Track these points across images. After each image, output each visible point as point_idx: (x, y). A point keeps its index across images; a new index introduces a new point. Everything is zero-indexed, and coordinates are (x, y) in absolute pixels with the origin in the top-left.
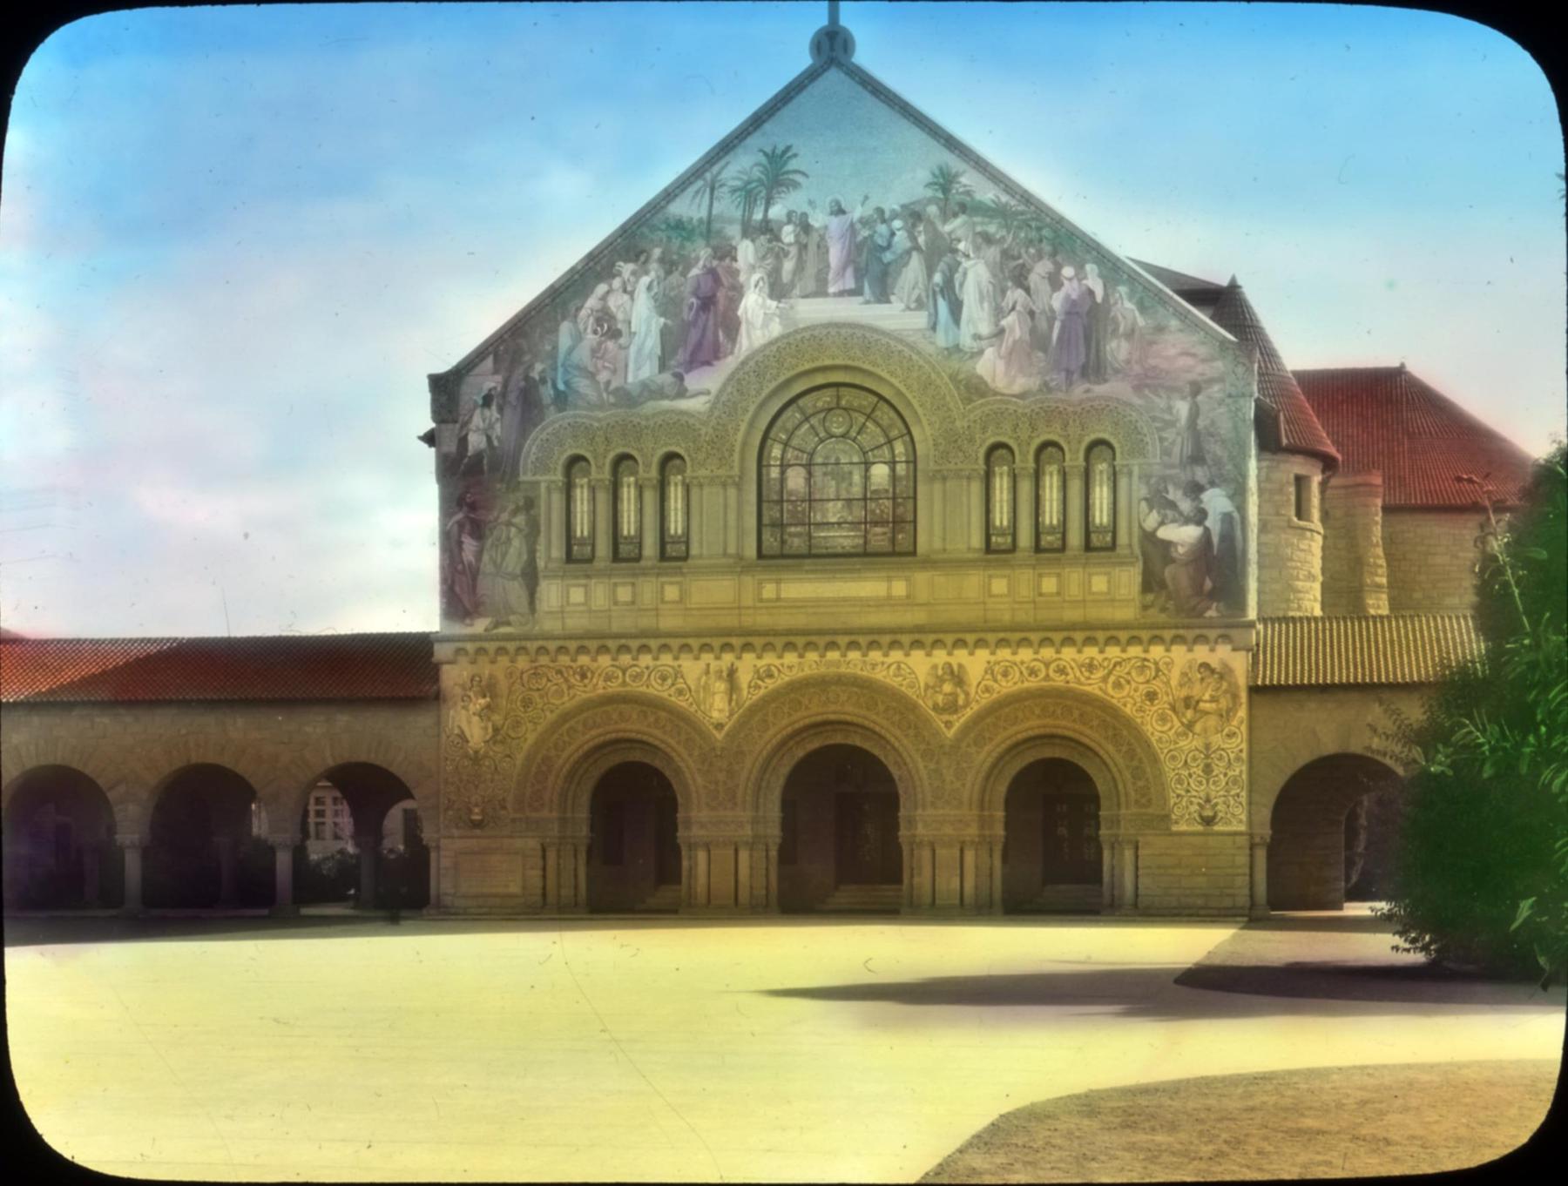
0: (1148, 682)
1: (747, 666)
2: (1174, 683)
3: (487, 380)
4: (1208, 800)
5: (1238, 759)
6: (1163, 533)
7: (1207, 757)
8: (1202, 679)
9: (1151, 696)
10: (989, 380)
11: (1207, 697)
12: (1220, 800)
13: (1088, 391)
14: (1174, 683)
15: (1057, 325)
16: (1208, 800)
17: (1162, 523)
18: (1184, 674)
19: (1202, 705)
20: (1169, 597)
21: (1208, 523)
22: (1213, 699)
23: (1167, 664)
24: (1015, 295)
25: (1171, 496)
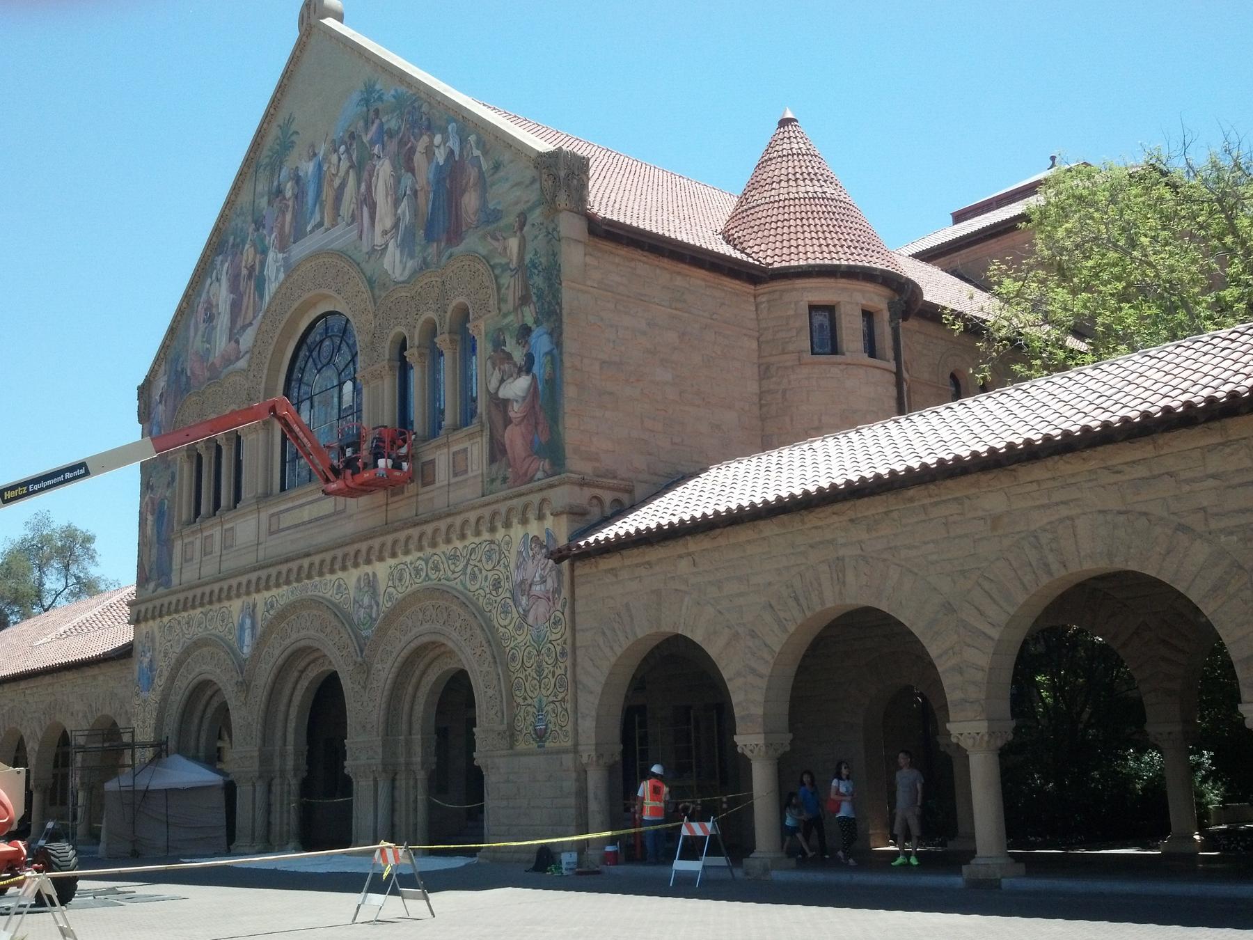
0: (494, 568)
1: (260, 598)
2: (512, 565)
3: (161, 383)
4: (540, 710)
5: (563, 654)
6: (501, 394)
7: (539, 652)
8: (534, 556)
9: (497, 585)
10: (390, 272)
11: (537, 579)
12: (550, 708)
13: (451, 256)
14: (512, 565)
15: (431, 195)
16: (540, 710)
17: (502, 381)
18: (520, 553)
19: (534, 588)
20: (509, 465)
21: (535, 369)
22: (543, 581)
23: (507, 544)
24: (407, 180)
25: (508, 349)
